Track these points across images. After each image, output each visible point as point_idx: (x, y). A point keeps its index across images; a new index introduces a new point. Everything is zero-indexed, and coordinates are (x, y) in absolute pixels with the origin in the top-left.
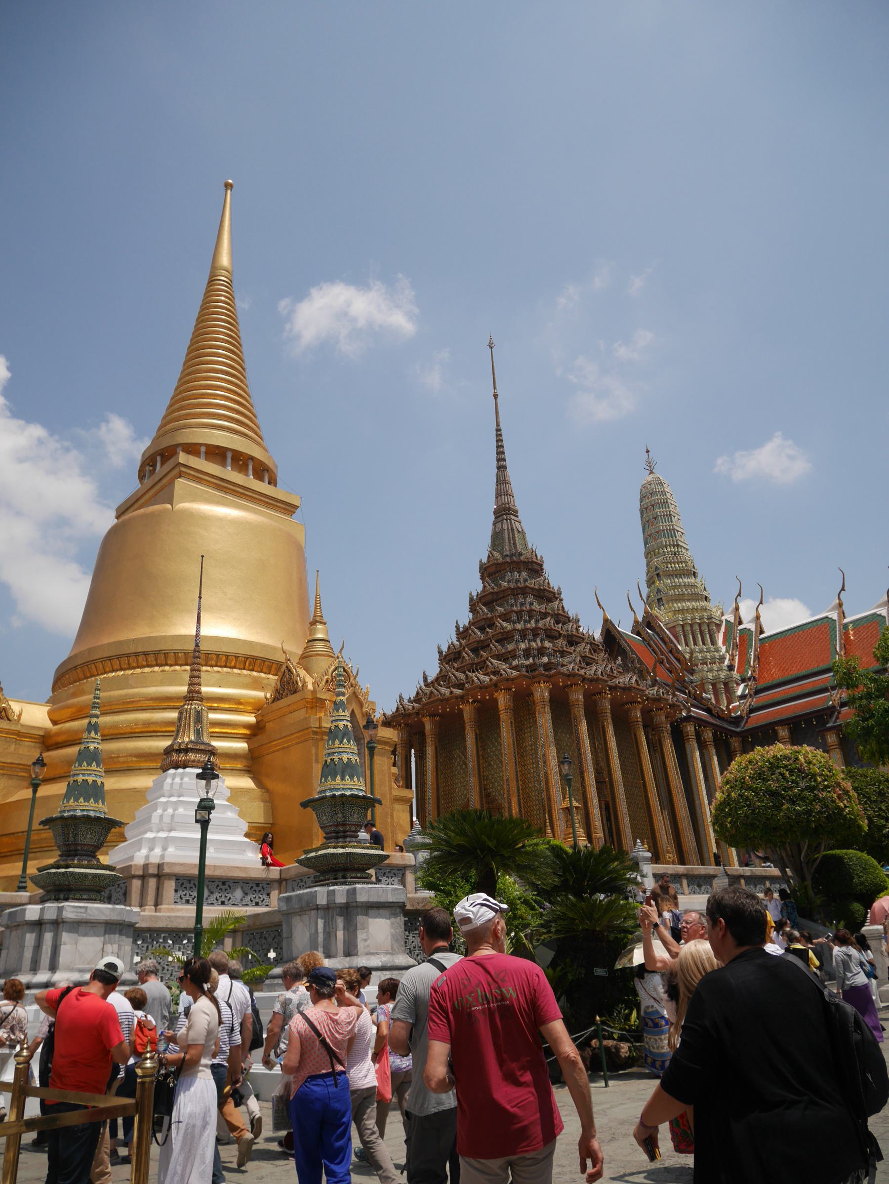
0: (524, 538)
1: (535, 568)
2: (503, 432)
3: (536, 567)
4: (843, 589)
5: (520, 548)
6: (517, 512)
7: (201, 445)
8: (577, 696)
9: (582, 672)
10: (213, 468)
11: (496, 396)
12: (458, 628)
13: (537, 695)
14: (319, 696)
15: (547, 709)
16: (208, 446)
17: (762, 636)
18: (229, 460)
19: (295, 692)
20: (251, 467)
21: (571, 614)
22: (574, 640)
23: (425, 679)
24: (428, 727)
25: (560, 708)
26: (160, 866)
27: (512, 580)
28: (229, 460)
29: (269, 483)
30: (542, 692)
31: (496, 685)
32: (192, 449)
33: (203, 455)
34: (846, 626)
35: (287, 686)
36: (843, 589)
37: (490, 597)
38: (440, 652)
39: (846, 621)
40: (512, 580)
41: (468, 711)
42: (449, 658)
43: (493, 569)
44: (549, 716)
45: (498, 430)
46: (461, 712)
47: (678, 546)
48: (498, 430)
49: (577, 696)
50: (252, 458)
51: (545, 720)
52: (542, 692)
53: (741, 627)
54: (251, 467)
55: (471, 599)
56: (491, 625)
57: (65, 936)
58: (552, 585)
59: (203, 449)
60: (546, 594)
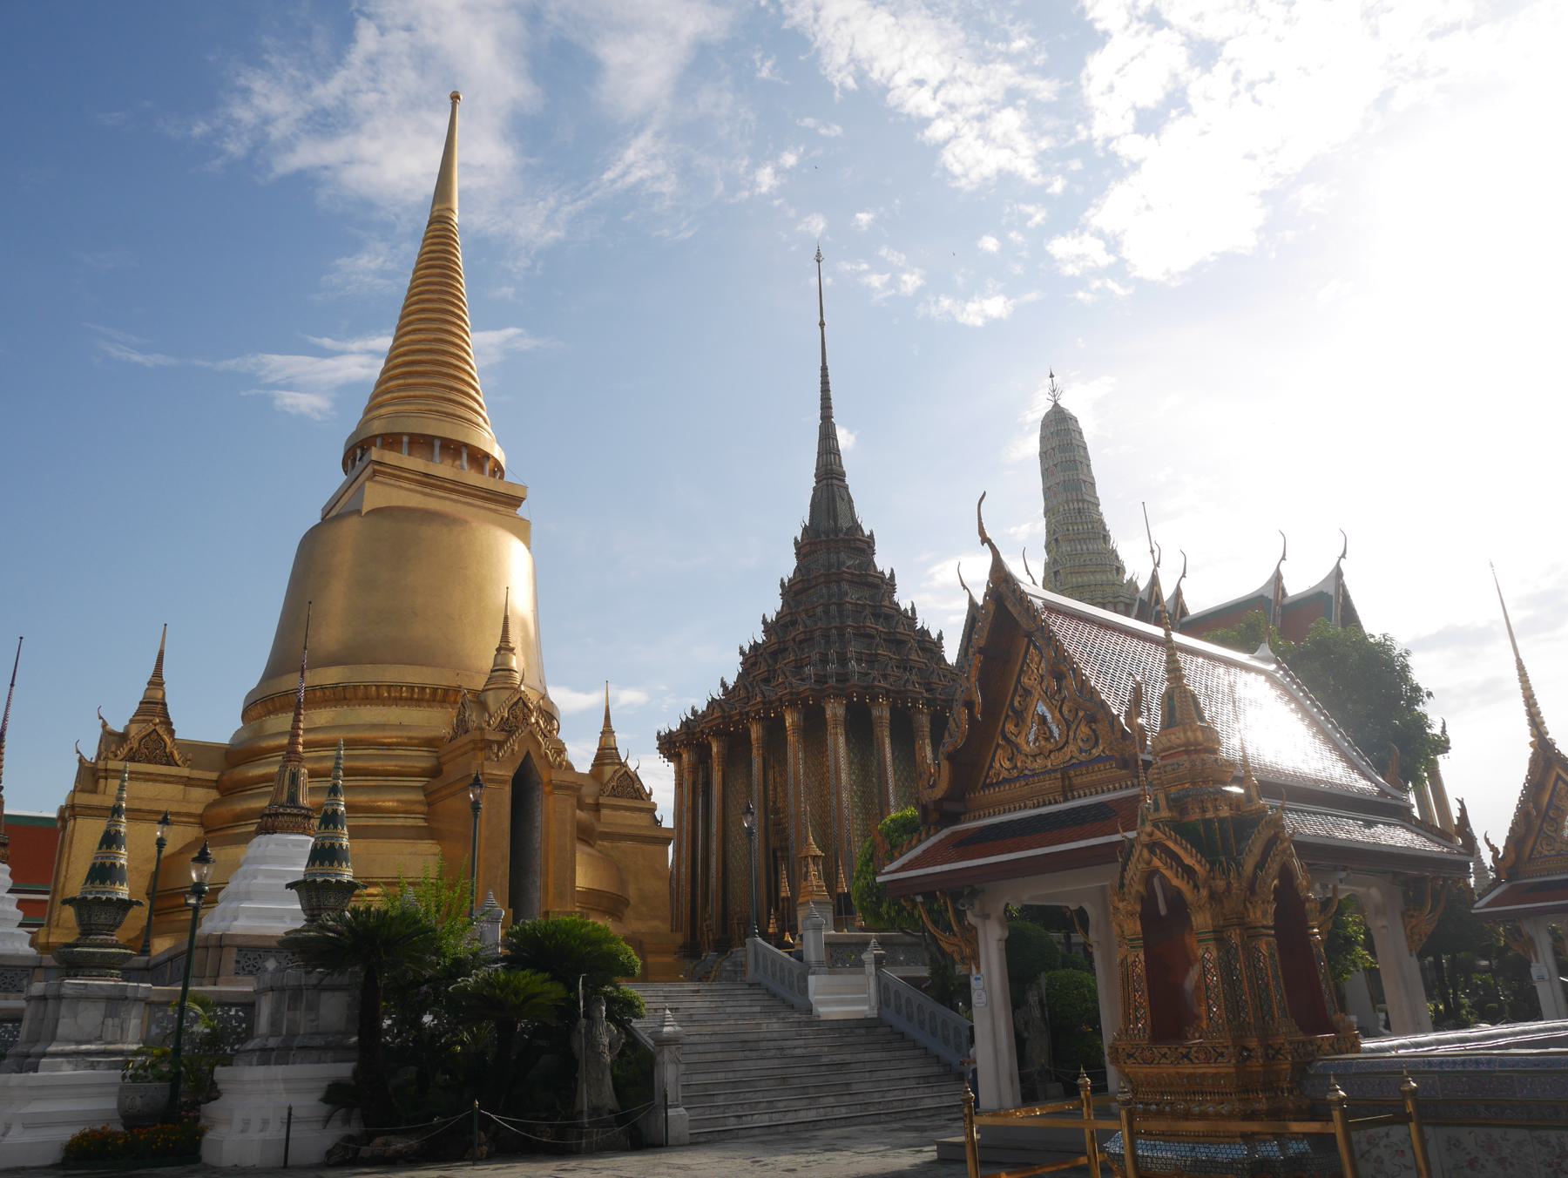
0: (851, 508)
1: (864, 546)
2: (830, 372)
3: (858, 544)
4: (1283, 558)
5: (844, 524)
6: (843, 474)
7: (402, 434)
8: (882, 712)
9: (883, 684)
10: (416, 463)
11: (822, 324)
12: (764, 622)
13: (829, 713)
14: (488, 737)
15: (841, 730)
16: (411, 435)
17: (1185, 619)
18: (437, 450)
19: (467, 732)
20: (465, 456)
21: (904, 604)
22: (896, 642)
23: (723, 684)
24: (715, 749)
25: (860, 727)
26: (221, 937)
27: (835, 560)
28: (437, 450)
29: (493, 473)
30: (834, 710)
31: (780, 699)
32: (391, 441)
33: (405, 448)
34: (1284, 607)
35: (461, 727)
36: (1283, 558)
37: (800, 586)
38: (742, 652)
39: (1286, 601)
40: (835, 560)
41: (755, 731)
42: (753, 658)
43: (808, 548)
44: (842, 740)
45: (824, 369)
46: (747, 731)
47: (1083, 501)
48: (824, 369)
49: (882, 712)
50: (466, 445)
51: (839, 743)
52: (834, 710)
53: (1159, 608)
54: (465, 456)
55: (782, 585)
56: (794, 623)
57: (63, 1010)
58: (880, 568)
59: (405, 439)
60: (870, 579)
